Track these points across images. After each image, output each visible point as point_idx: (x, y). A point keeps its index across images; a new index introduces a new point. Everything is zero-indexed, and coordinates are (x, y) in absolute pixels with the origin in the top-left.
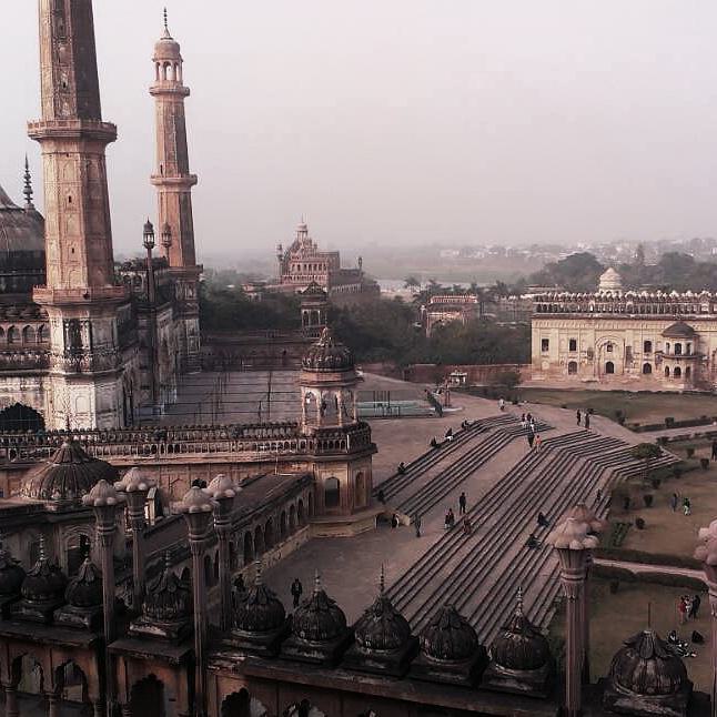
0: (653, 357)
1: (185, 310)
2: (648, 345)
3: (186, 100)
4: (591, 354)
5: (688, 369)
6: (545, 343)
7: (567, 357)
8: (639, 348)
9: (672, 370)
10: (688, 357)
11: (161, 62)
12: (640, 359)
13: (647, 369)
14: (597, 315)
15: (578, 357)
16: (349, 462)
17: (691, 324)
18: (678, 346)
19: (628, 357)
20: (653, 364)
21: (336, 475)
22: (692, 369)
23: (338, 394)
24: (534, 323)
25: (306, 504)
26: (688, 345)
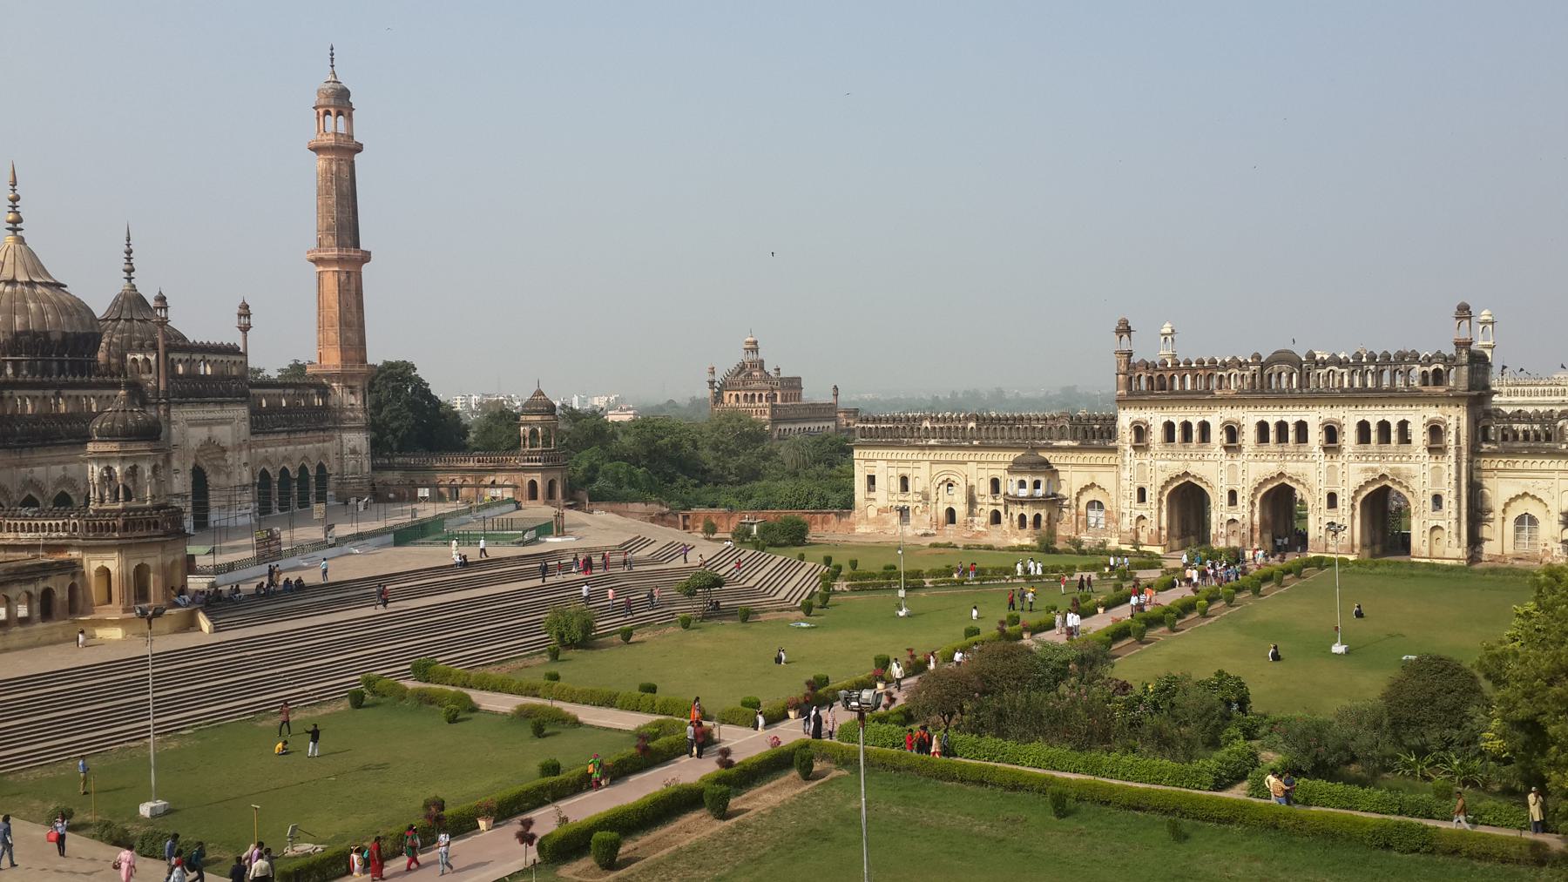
0: (1001, 501)
1: (342, 421)
2: (995, 483)
3: (357, 157)
4: (926, 497)
5: (1037, 518)
6: (871, 480)
7: (898, 499)
8: (984, 488)
9: (1016, 517)
10: (1032, 500)
11: (321, 111)
12: (986, 505)
13: (996, 518)
14: (932, 442)
15: (911, 500)
16: (120, 548)
17: (1046, 455)
18: (1022, 484)
19: (972, 502)
20: (1001, 509)
21: (107, 564)
22: (1044, 518)
23: (117, 469)
24: (856, 453)
25: (61, 595)
26: (1037, 485)
